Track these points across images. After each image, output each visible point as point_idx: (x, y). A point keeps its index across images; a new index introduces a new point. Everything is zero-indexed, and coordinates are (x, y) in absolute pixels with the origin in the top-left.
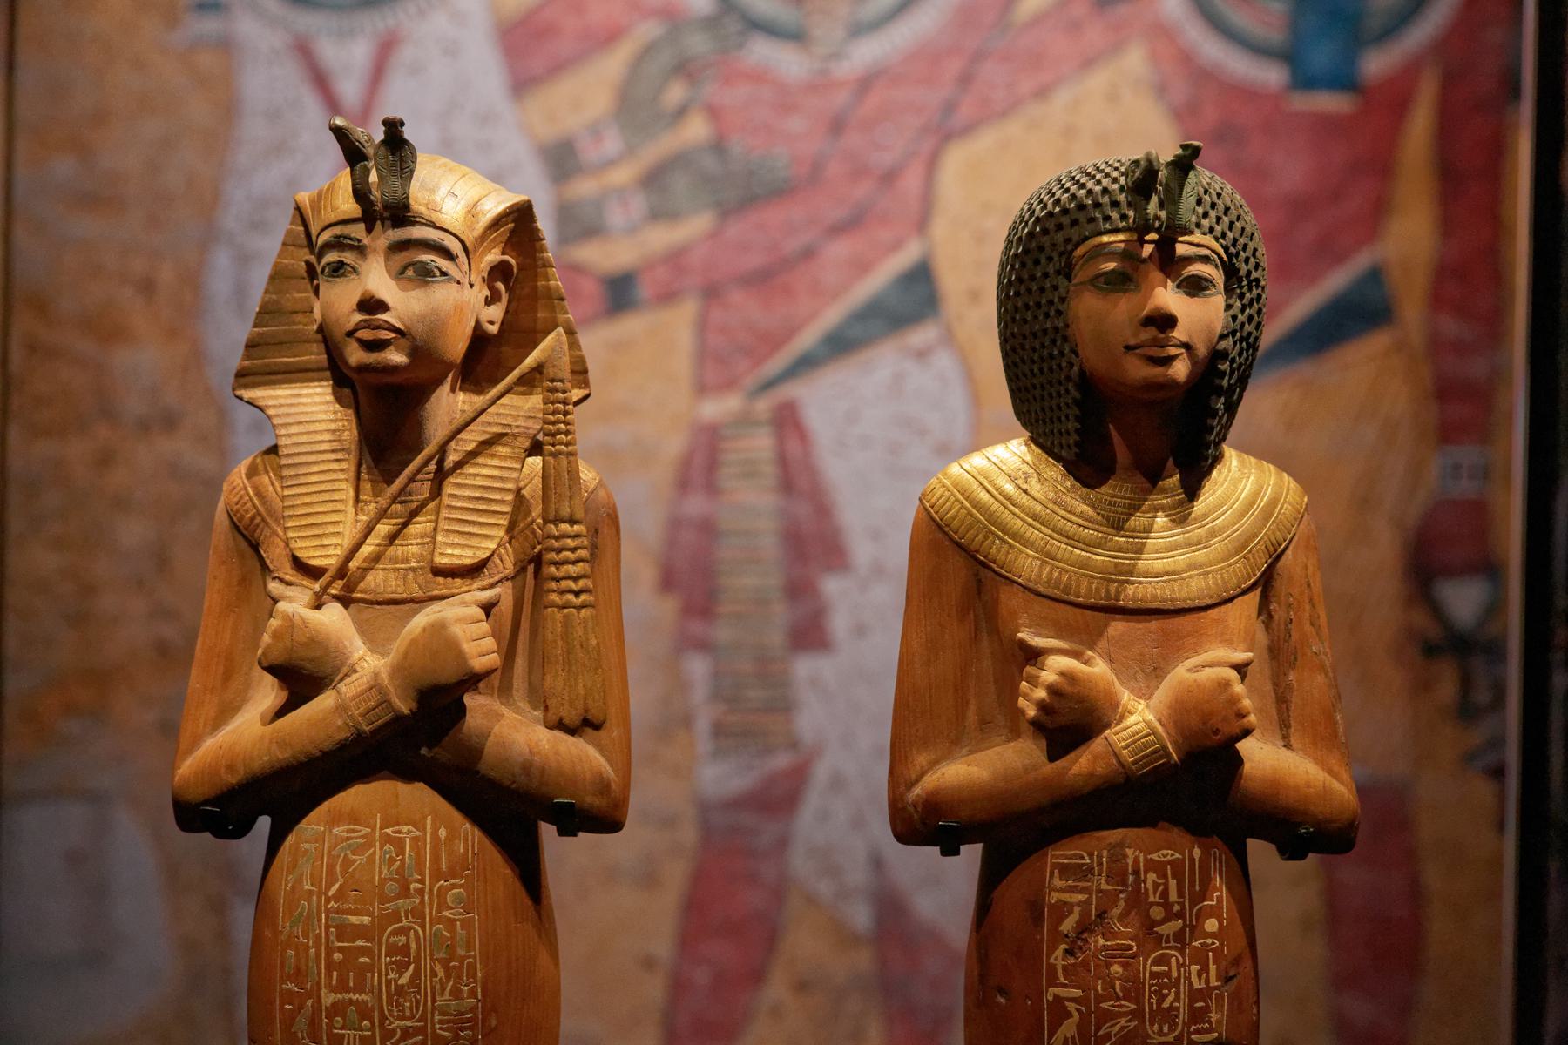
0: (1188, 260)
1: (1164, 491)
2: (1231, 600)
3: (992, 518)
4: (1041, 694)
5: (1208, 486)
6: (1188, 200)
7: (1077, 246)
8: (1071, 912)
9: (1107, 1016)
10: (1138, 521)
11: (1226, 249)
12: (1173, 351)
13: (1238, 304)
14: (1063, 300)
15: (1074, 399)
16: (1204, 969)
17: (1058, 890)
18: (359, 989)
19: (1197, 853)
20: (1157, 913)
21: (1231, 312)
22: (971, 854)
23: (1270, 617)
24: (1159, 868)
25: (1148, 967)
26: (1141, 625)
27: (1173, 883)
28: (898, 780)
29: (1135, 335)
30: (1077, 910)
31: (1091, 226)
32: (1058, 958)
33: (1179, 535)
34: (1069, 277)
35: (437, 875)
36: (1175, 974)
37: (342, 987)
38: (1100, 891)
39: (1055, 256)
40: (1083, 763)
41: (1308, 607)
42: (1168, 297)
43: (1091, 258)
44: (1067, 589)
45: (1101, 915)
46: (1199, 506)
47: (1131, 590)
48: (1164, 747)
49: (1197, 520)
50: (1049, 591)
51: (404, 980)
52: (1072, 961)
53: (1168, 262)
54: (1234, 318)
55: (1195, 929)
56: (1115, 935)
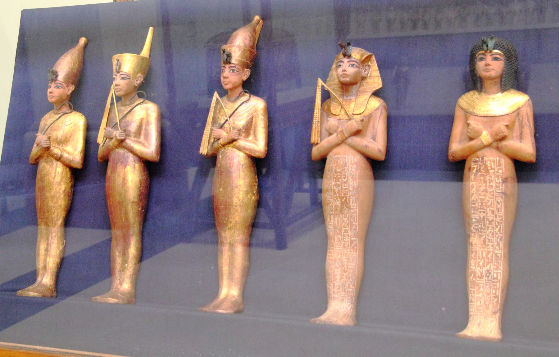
18: (338, 181)
37: (336, 181)
45: (480, 169)
51: (345, 180)
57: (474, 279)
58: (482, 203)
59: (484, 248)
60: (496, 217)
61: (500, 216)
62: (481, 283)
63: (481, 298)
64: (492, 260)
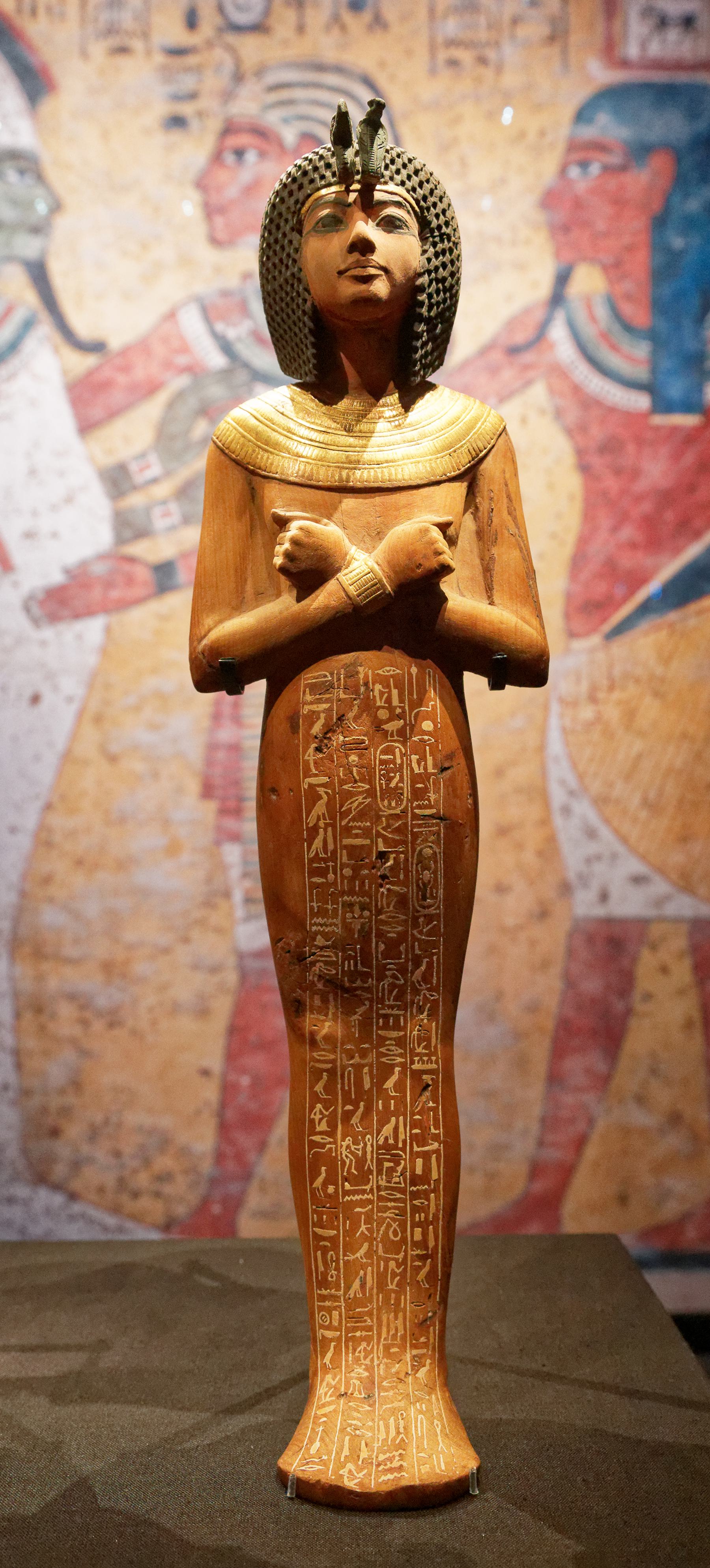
0: (384, 204)
2: (438, 483)
3: (258, 435)
4: (287, 545)
7: (303, 204)
8: (318, 718)
9: (350, 794)
10: (363, 426)
11: (417, 201)
12: (373, 271)
13: (432, 250)
14: (297, 250)
15: (310, 331)
16: (422, 759)
19: (414, 670)
20: (383, 714)
21: (426, 256)
23: (477, 509)
24: (384, 681)
25: (377, 755)
26: (367, 501)
27: (395, 692)
28: (194, 638)
29: (344, 261)
30: (322, 716)
31: (312, 186)
32: (311, 755)
34: (300, 232)
36: (399, 761)
38: (340, 700)
39: (290, 217)
41: (505, 500)
42: (366, 228)
43: (313, 210)
44: (310, 478)
45: (340, 718)
47: (358, 473)
48: (380, 581)
49: (410, 425)
50: (297, 480)
52: (321, 755)
53: (369, 206)
54: (429, 260)
56: (351, 733)
57: (331, 1189)
58: (356, 869)
59: (364, 1054)
60: (415, 925)
61: (429, 918)
62: (362, 1203)
63: (363, 1267)
64: (401, 1101)
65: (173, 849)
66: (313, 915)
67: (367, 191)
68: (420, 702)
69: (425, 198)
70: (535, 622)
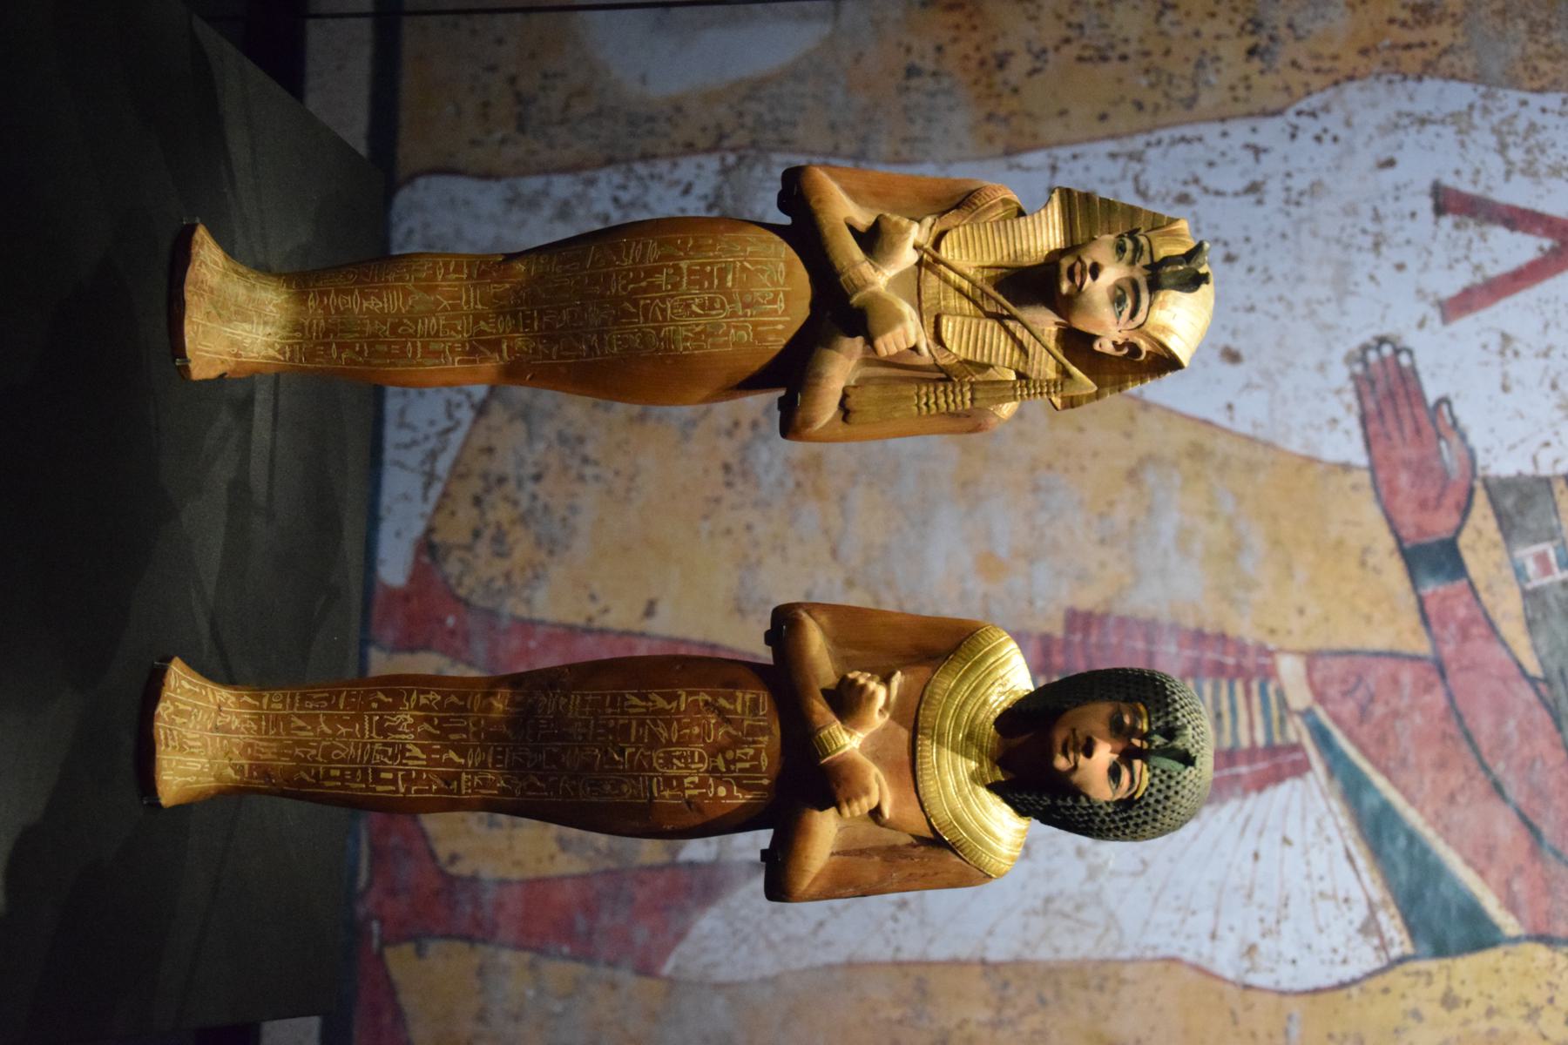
1: (993, 769)
2: (923, 809)
5: (998, 799)
6: (1167, 764)
11: (1142, 798)
12: (1071, 756)
16: (697, 786)
17: (743, 698)
18: (689, 283)
19: (766, 782)
20: (730, 755)
22: (765, 654)
24: (756, 757)
25: (698, 749)
27: (747, 765)
28: (811, 608)
33: (964, 776)
35: (755, 325)
37: (691, 272)
40: (820, 708)
42: (1104, 754)
44: (928, 703)
45: (729, 721)
46: (983, 792)
51: (694, 308)
55: (720, 780)
56: (716, 729)
57: (375, 705)
59: (477, 735)
62: (362, 730)
63: (314, 729)
64: (438, 763)
65: (989, 565)
66: (583, 696)
67: (1143, 755)
68: (741, 787)
69: (1148, 805)
70: (813, 890)
